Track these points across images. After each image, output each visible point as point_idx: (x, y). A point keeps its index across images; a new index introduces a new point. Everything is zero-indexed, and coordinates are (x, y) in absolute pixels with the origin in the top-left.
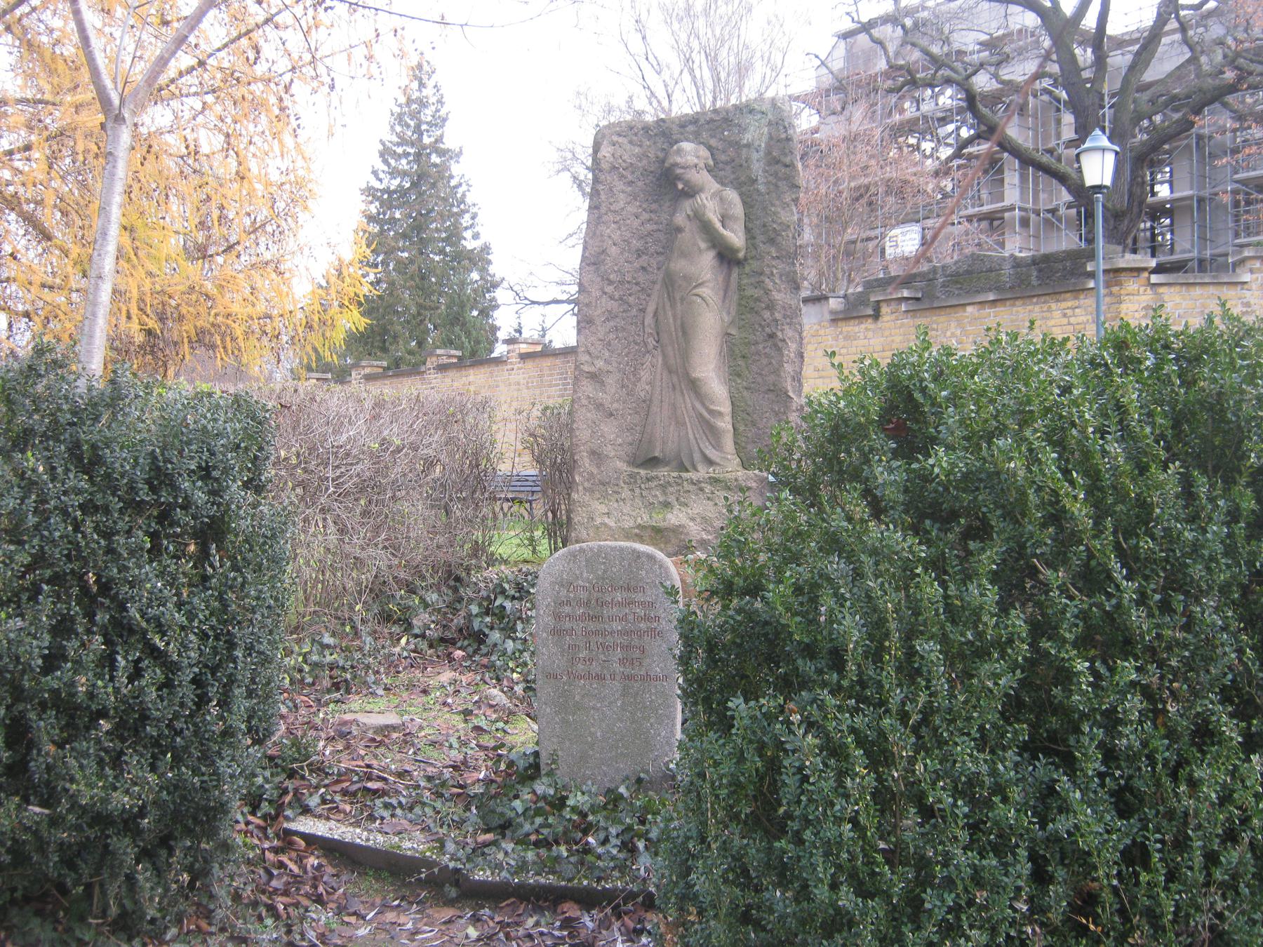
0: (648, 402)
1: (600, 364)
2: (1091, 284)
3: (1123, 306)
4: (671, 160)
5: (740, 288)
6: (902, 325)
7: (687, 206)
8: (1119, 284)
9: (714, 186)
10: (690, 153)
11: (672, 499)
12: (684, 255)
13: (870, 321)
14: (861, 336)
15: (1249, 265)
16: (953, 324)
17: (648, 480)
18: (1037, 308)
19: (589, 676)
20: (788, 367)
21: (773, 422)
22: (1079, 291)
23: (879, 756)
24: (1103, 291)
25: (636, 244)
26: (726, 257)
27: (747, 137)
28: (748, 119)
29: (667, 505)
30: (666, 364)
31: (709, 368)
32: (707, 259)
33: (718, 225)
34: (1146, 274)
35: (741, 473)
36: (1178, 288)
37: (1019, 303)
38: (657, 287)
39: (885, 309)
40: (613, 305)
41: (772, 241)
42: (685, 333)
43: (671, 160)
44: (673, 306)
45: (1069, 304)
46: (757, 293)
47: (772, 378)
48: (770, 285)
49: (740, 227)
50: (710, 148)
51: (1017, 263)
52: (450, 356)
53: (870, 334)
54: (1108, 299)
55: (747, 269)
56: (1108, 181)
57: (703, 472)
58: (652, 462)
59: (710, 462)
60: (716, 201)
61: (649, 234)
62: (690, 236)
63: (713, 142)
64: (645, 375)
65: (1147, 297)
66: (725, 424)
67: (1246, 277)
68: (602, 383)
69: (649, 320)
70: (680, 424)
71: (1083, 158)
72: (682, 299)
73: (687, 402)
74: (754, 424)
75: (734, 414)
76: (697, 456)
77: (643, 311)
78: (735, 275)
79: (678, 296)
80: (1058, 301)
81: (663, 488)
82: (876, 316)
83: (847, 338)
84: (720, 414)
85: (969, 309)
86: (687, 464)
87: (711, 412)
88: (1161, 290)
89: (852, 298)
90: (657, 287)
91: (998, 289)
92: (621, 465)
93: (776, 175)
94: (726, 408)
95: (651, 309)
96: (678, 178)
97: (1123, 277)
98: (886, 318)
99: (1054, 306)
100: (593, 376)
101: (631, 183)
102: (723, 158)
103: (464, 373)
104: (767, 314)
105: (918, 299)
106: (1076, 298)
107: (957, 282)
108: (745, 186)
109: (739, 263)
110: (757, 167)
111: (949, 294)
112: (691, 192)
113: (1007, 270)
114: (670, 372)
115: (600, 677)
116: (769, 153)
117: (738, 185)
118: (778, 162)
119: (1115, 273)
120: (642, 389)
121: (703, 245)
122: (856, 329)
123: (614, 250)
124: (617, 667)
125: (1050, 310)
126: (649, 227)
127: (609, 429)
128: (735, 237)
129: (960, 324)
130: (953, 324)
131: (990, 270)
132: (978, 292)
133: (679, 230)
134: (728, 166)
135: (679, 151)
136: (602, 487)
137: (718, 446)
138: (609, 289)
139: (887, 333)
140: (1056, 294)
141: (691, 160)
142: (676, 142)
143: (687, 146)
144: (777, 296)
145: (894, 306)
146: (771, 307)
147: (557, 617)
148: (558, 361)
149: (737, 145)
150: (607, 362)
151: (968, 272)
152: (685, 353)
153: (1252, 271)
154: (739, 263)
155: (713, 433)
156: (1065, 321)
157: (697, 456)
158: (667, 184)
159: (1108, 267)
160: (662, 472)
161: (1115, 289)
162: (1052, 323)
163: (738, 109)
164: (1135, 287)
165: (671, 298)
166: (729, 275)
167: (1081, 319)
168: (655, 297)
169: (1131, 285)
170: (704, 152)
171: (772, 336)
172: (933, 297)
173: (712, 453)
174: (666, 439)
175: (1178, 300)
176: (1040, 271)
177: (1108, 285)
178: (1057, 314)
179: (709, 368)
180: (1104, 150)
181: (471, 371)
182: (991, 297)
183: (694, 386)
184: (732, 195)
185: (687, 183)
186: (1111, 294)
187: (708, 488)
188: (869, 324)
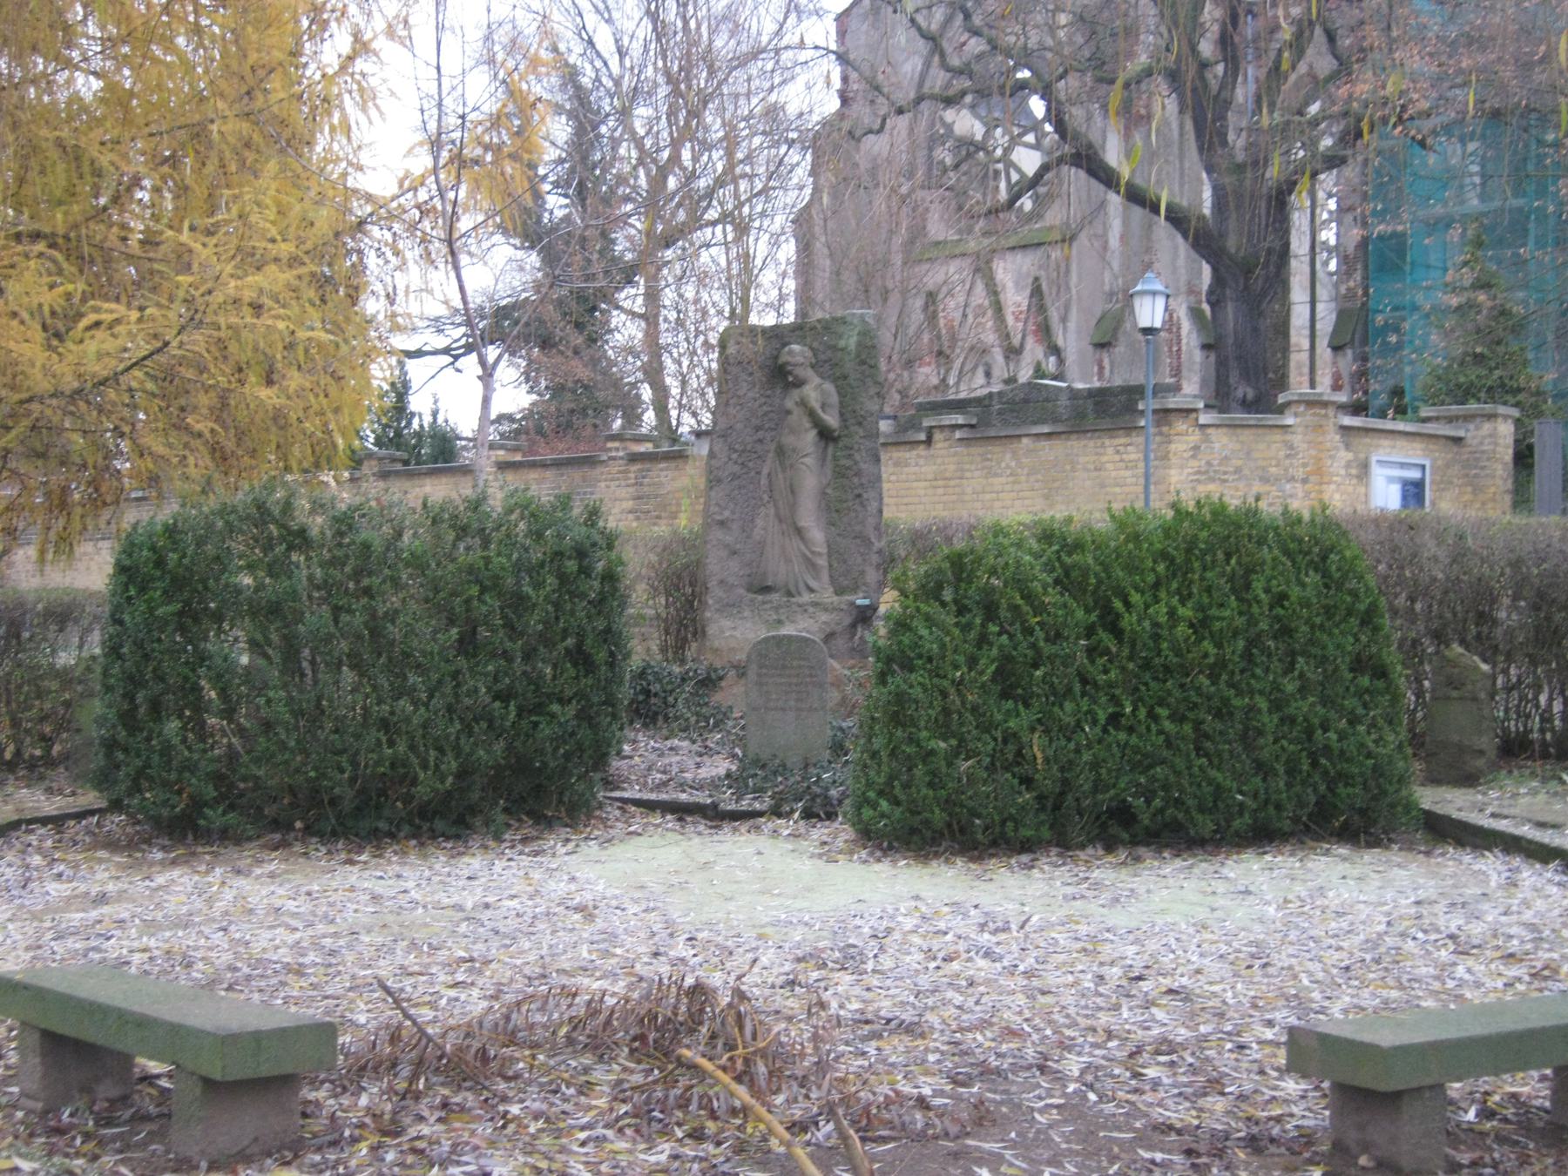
0: (762, 544)
1: (727, 513)
2: (1142, 423)
3: (1173, 447)
4: (782, 359)
5: (835, 458)
6: (955, 454)
7: (795, 394)
8: (1170, 425)
9: (817, 380)
10: (797, 351)
11: (783, 618)
12: (793, 431)
13: (922, 447)
14: (913, 462)
15: (1293, 409)
16: (1008, 456)
17: (764, 603)
18: (1091, 444)
19: (776, 709)
20: (871, 521)
21: (859, 560)
22: (1131, 429)
23: (944, 695)
24: (1152, 430)
25: (754, 421)
26: (825, 435)
27: (842, 343)
28: (842, 329)
29: (780, 622)
30: (778, 516)
31: (810, 519)
32: (812, 435)
33: (820, 411)
34: (1194, 415)
35: (836, 598)
36: (1225, 430)
37: (1074, 436)
38: (771, 455)
39: (938, 436)
40: (736, 468)
41: (860, 424)
42: (793, 492)
43: (782, 359)
44: (784, 471)
45: (1123, 441)
46: (848, 463)
47: (858, 528)
48: (857, 457)
49: (835, 412)
50: (811, 348)
51: (1074, 394)
52: (394, 460)
53: (922, 462)
54: (1158, 439)
55: (841, 444)
56: (1158, 324)
57: (806, 597)
58: (766, 589)
59: (811, 590)
60: (816, 390)
61: (765, 414)
62: (798, 418)
63: (815, 345)
64: (759, 522)
65: (1195, 437)
66: (822, 562)
67: (1289, 421)
68: (729, 529)
69: (764, 481)
70: (788, 561)
71: (1137, 302)
72: (792, 466)
73: (795, 544)
74: (845, 562)
75: (829, 555)
76: (801, 585)
77: (758, 473)
78: (830, 449)
79: (788, 463)
80: (1112, 437)
81: (777, 609)
82: (929, 442)
83: (896, 464)
84: (820, 554)
85: (1025, 441)
86: (793, 590)
87: (813, 553)
88: (1210, 431)
89: (903, 421)
90: (771, 455)
91: (1056, 420)
92: (742, 591)
93: (863, 373)
94: (824, 550)
95: (765, 471)
96: (790, 373)
97: (1172, 417)
98: (939, 445)
99: (1107, 442)
100: (722, 523)
101: (751, 374)
102: (823, 357)
103: (417, 482)
104: (856, 480)
105: (972, 426)
106: (1128, 435)
107: (1012, 411)
108: (840, 380)
109: (835, 440)
110: (849, 366)
111: (1005, 423)
112: (799, 383)
113: (1064, 401)
114: (781, 521)
115: (783, 709)
116: (858, 356)
117: (835, 380)
118: (863, 363)
119: (1164, 415)
120: (758, 533)
121: (808, 425)
122: (907, 455)
123: (739, 426)
124: (792, 703)
125: (1103, 446)
126: (765, 408)
127: (734, 565)
128: (832, 420)
129: (1014, 453)
130: (1008, 456)
131: (1047, 400)
132: (1035, 423)
133: (789, 412)
134: (828, 365)
135: (791, 352)
136: (728, 607)
137: (817, 578)
138: (735, 456)
139: (939, 461)
140: (1111, 431)
141: (800, 359)
142: (785, 345)
143: (796, 347)
144: (863, 466)
145: (947, 433)
146: (858, 474)
147: (759, 675)
148: (549, 474)
149: (834, 348)
150: (733, 513)
151: (1026, 401)
152: (793, 507)
153: (1296, 415)
154: (835, 440)
155: (812, 566)
156: (1117, 457)
157: (801, 585)
158: (780, 376)
159: (1157, 407)
160: (775, 597)
161: (1165, 429)
162: (1105, 459)
163: (835, 320)
164: (1184, 427)
165: (781, 463)
166: (826, 448)
167: (1133, 456)
168: (769, 462)
169: (1181, 426)
170: (809, 354)
171: (859, 496)
172: (988, 424)
173: (813, 584)
174: (778, 571)
175: (1225, 440)
176: (1096, 404)
177: (1158, 424)
178: (1110, 450)
179: (810, 519)
180: (1154, 293)
181: (428, 481)
182: (1046, 429)
183: (800, 532)
184: (829, 387)
185: (796, 377)
186: (1161, 434)
187: (811, 610)
188: (921, 450)
